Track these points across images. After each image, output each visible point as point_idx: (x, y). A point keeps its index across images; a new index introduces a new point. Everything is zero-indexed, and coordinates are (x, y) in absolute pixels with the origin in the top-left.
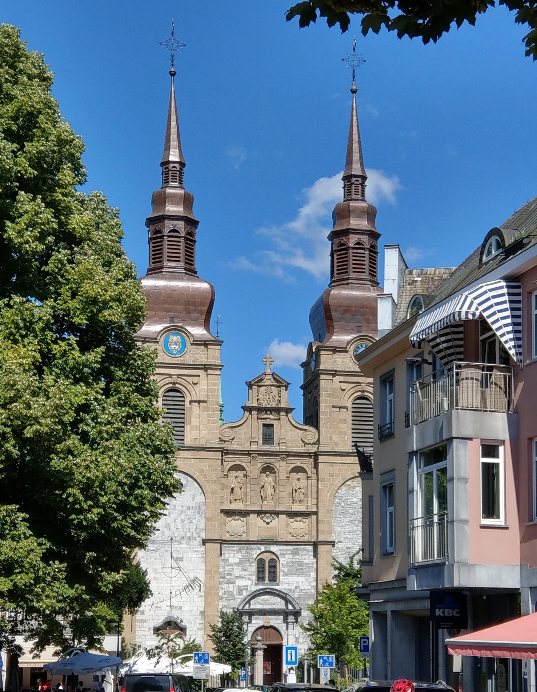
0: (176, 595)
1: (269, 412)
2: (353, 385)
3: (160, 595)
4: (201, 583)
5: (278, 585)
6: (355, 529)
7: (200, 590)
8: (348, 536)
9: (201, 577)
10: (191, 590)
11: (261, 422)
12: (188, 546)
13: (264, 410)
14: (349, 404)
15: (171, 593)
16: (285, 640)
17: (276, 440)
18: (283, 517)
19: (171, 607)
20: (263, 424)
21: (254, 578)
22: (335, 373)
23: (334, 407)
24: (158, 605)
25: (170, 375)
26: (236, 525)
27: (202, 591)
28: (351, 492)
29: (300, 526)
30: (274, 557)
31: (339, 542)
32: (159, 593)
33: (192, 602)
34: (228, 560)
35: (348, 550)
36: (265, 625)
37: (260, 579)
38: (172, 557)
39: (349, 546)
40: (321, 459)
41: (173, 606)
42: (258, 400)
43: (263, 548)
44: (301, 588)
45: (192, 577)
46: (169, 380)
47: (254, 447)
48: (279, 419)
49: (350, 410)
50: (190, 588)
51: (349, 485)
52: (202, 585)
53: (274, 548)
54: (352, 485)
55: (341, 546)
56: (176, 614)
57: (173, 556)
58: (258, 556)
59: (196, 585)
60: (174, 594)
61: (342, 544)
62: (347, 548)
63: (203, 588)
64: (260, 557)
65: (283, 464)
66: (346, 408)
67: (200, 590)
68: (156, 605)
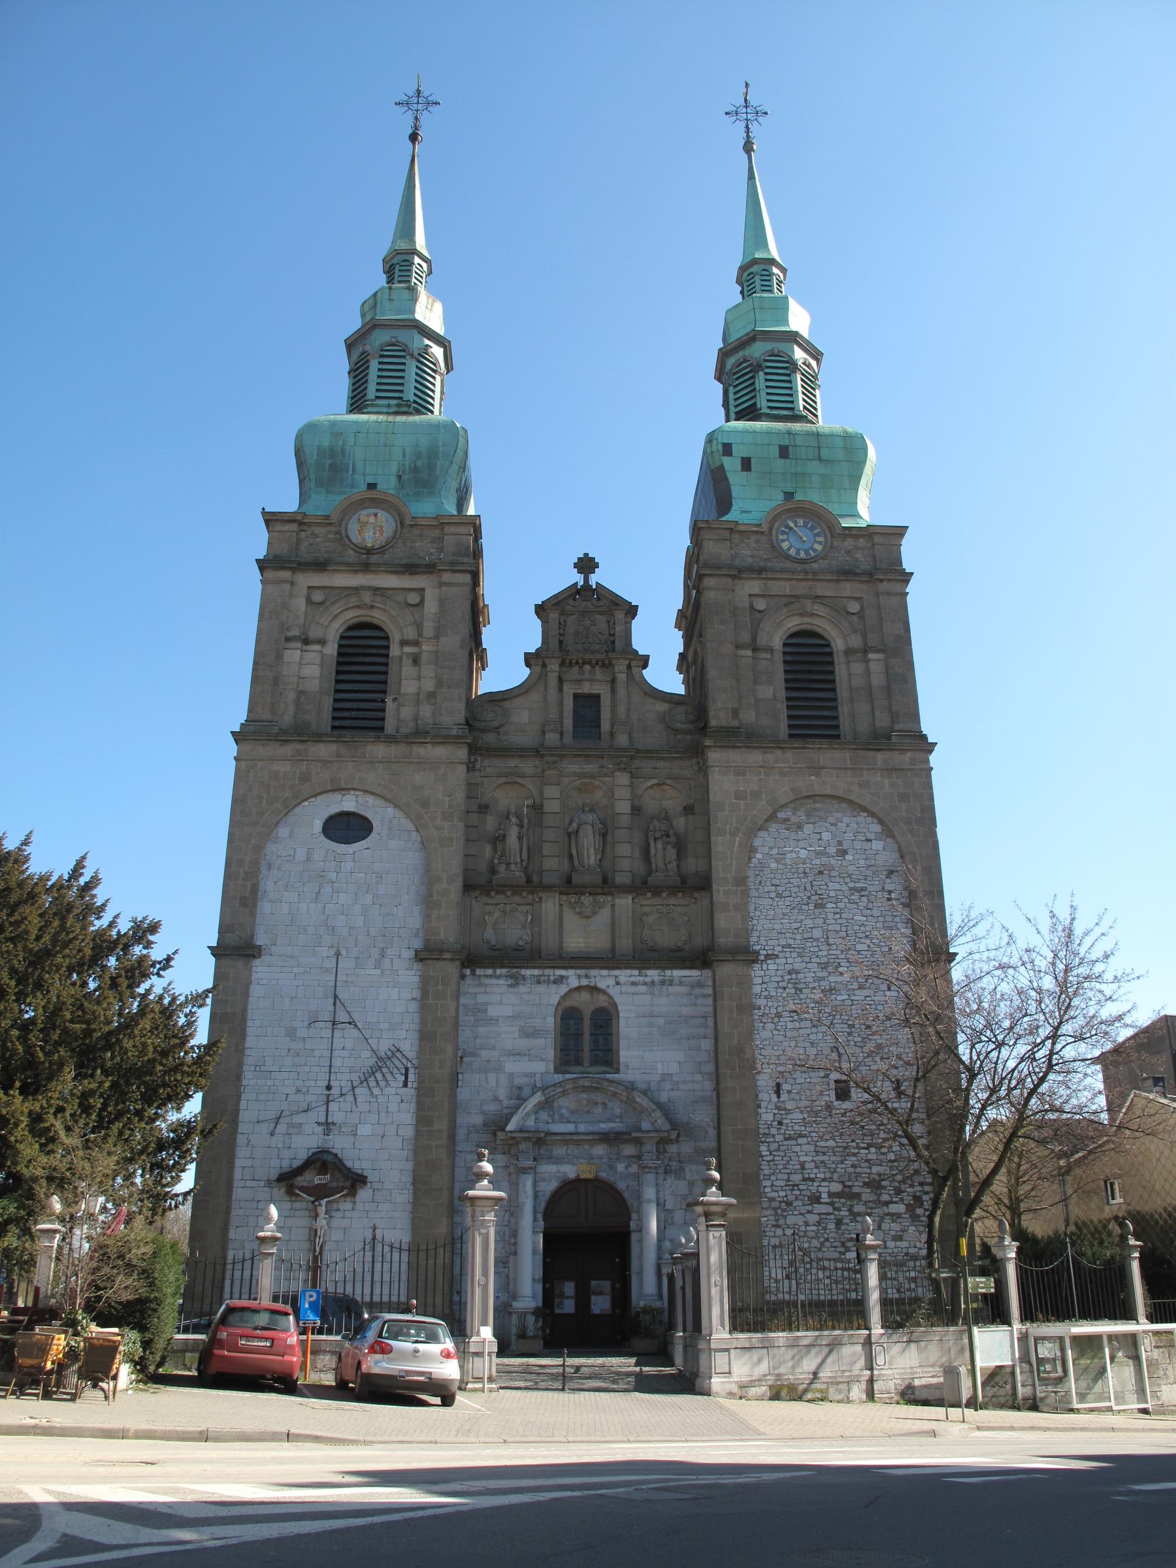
0: (342, 1095)
1: (587, 667)
2: (785, 600)
3: (300, 1097)
4: (409, 1065)
5: (617, 1071)
6: (809, 923)
7: (405, 1085)
8: (791, 942)
9: (409, 1047)
10: (382, 1084)
11: (569, 690)
12: (378, 972)
13: (577, 663)
14: (777, 643)
15: (329, 1088)
16: (634, 1216)
17: (605, 726)
18: (625, 902)
19: (328, 1126)
20: (576, 696)
21: (550, 1054)
22: (738, 573)
23: (737, 647)
24: (297, 1119)
25: (357, 590)
26: (508, 925)
27: (410, 1084)
28: (793, 836)
29: (668, 921)
30: (602, 1001)
31: (768, 957)
32: (299, 1091)
33: (383, 1115)
34: (485, 1011)
35: (794, 976)
36: (583, 1176)
37: (568, 1057)
38: (336, 997)
39: (797, 966)
40: (713, 756)
41: (334, 1124)
42: (561, 642)
43: (573, 978)
44: (675, 1078)
45: (384, 1046)
46: (354, 601)
47: (552, 738)
48: (613, 681)
49: (779, 658)
50: (379, 1076)
51: (787, 820)
52: (411, 1071)
53: (603, 979)
54: (794, 819)
55: (775, 967)
56: (339, 1144)
57: (342, 995)
58: (564, 997)
59: (395, 1071)
60: (335, 1091)
61: (778, 961)
62: (790, 973)
63: (411, 1077)
64: (568, 1004)
65: (623, 779)
66: (771, 650)
67: (405, 1085)
68: (288, 1120)
